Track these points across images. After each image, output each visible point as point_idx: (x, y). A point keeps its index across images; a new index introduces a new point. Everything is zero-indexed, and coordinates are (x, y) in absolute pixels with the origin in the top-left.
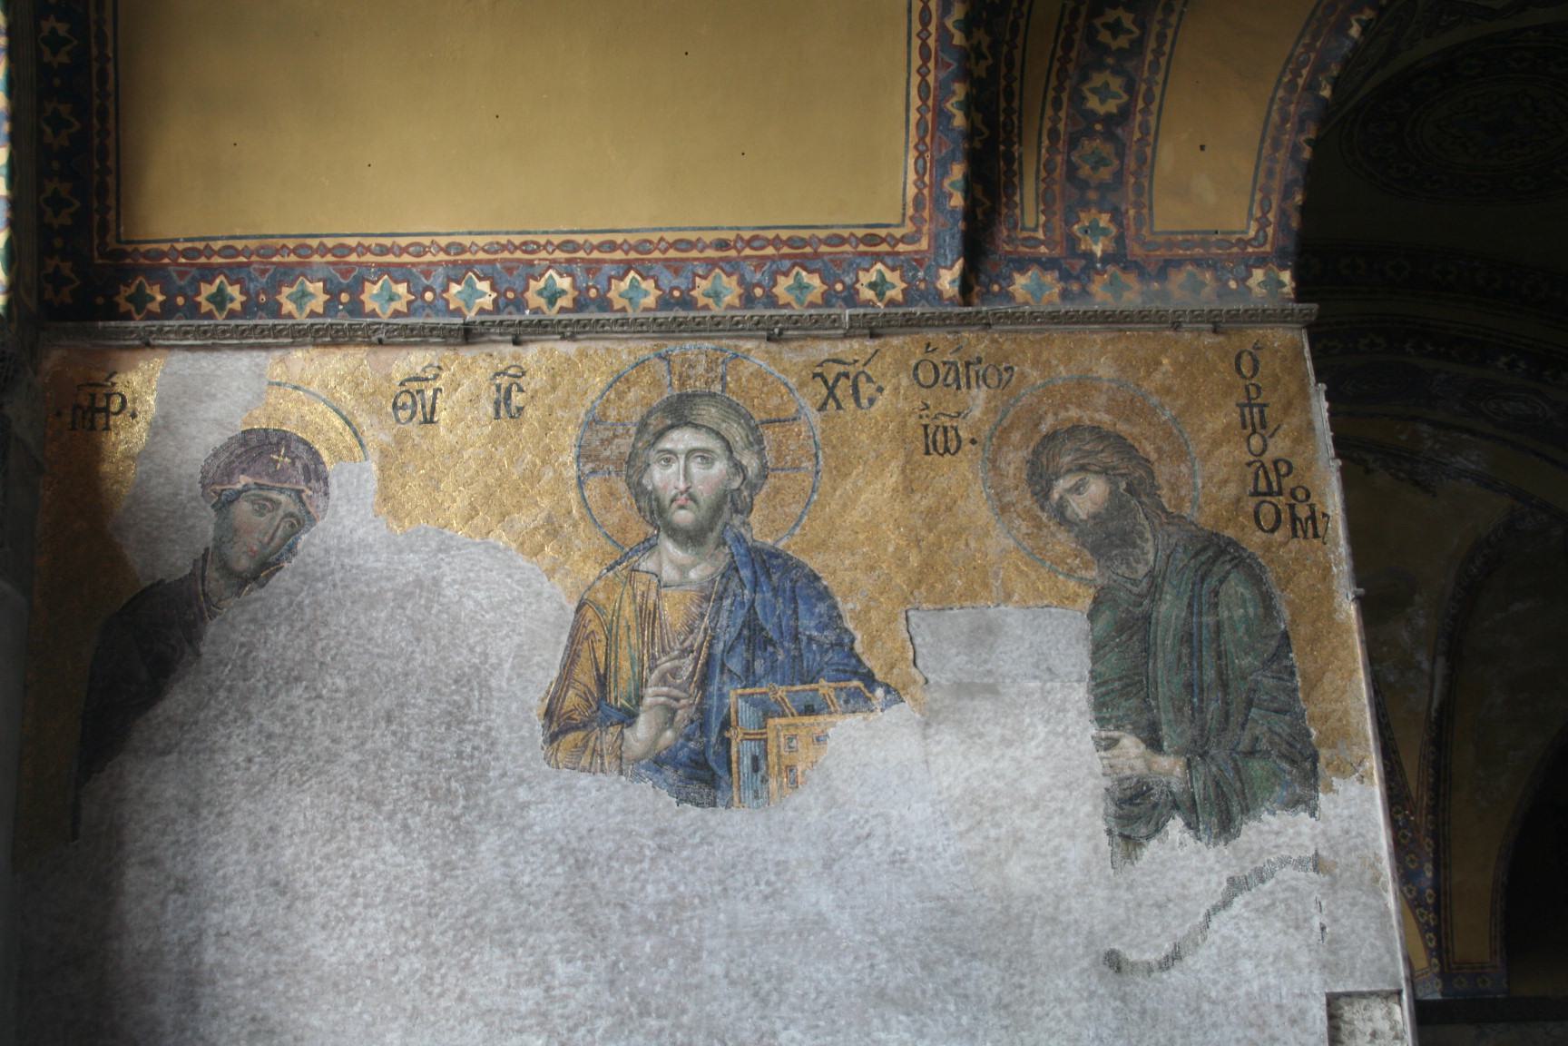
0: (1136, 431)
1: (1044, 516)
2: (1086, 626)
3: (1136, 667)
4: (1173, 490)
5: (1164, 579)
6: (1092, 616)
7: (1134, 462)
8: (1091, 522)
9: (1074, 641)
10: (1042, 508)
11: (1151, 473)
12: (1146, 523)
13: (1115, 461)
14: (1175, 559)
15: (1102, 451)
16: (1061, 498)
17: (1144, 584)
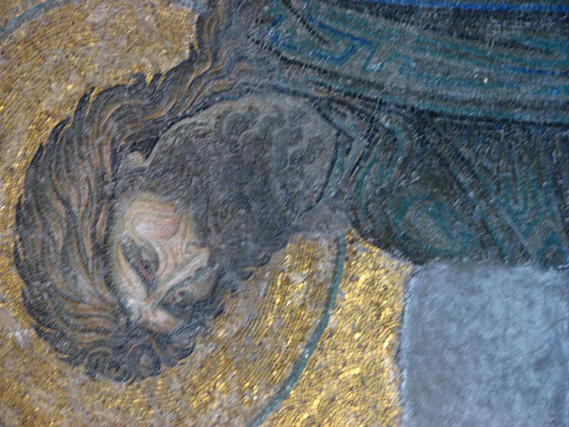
0: (22, 122)
1: (202, 351)
2: (440, 268)
3: (533, 153)
4: (142, 43)
5: (335, 76)
6: (417, 254)
7: (88, 130)
8: (214, 238)
9: (475, 301)
10: (186, 352)
11: (110, 92)
12: (215, 110)
13: (85, 172)
14: (291, 47)
15: (66, 203)
16: (165, 305)
17: (349, 122)
